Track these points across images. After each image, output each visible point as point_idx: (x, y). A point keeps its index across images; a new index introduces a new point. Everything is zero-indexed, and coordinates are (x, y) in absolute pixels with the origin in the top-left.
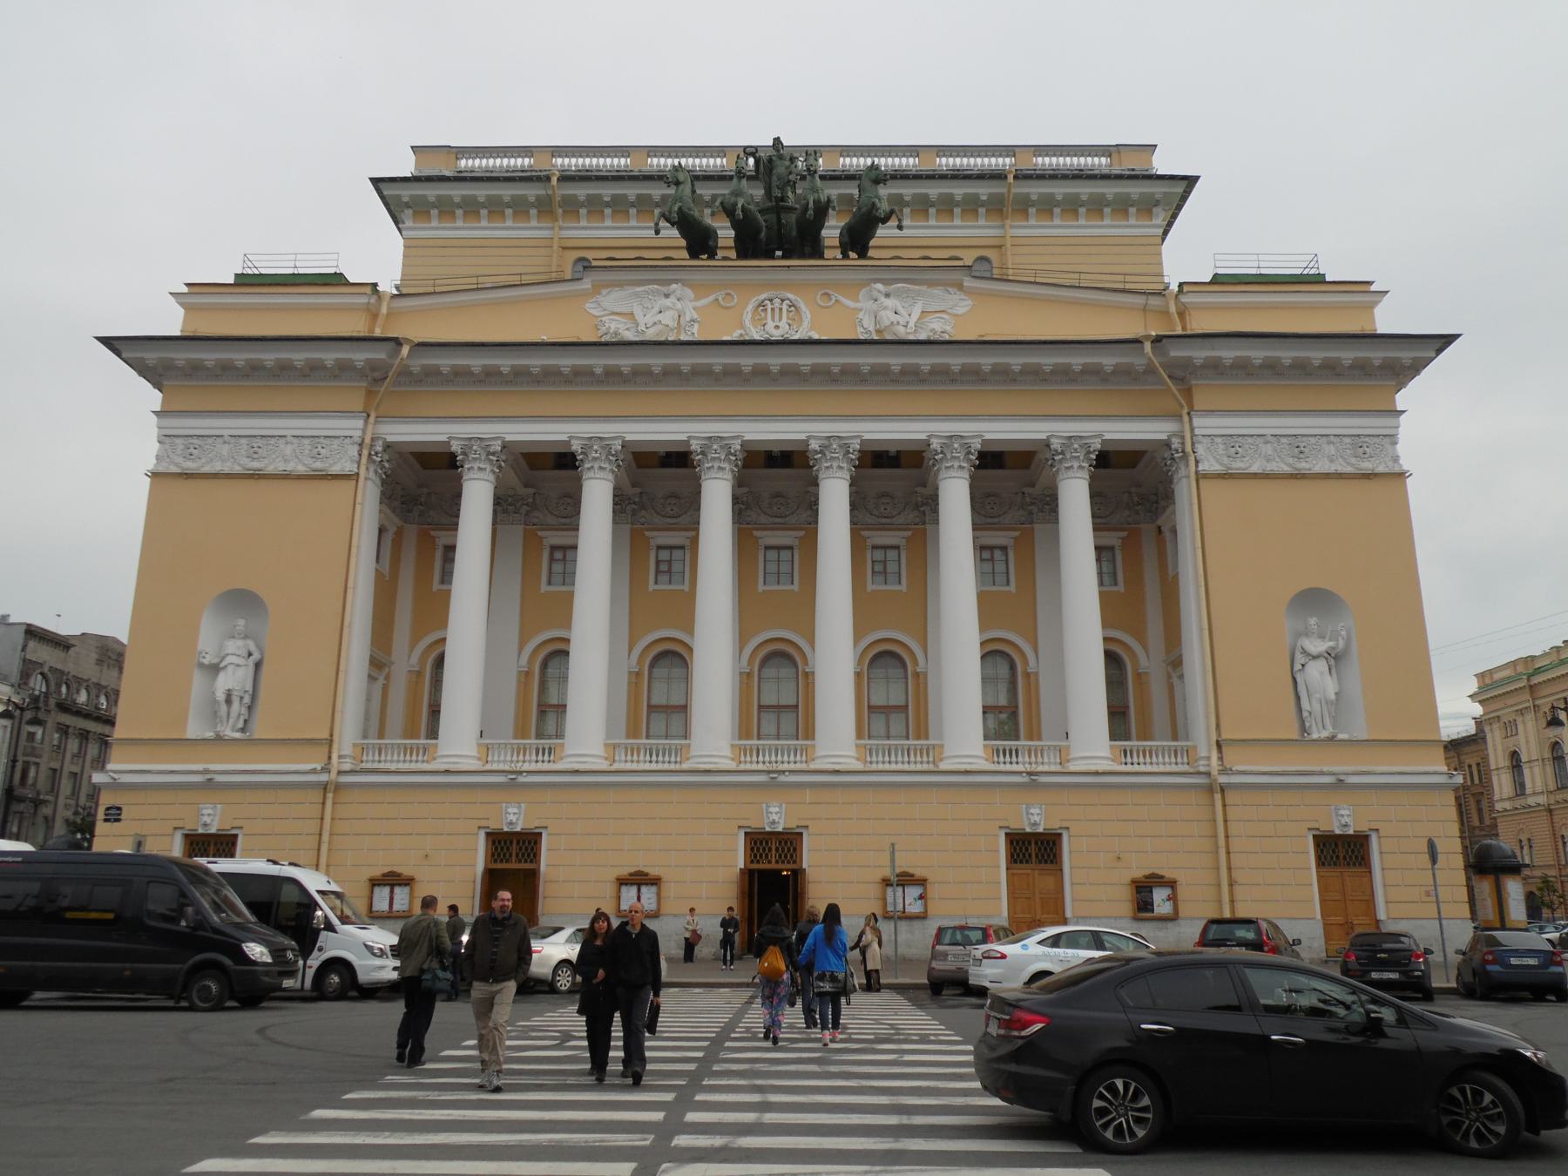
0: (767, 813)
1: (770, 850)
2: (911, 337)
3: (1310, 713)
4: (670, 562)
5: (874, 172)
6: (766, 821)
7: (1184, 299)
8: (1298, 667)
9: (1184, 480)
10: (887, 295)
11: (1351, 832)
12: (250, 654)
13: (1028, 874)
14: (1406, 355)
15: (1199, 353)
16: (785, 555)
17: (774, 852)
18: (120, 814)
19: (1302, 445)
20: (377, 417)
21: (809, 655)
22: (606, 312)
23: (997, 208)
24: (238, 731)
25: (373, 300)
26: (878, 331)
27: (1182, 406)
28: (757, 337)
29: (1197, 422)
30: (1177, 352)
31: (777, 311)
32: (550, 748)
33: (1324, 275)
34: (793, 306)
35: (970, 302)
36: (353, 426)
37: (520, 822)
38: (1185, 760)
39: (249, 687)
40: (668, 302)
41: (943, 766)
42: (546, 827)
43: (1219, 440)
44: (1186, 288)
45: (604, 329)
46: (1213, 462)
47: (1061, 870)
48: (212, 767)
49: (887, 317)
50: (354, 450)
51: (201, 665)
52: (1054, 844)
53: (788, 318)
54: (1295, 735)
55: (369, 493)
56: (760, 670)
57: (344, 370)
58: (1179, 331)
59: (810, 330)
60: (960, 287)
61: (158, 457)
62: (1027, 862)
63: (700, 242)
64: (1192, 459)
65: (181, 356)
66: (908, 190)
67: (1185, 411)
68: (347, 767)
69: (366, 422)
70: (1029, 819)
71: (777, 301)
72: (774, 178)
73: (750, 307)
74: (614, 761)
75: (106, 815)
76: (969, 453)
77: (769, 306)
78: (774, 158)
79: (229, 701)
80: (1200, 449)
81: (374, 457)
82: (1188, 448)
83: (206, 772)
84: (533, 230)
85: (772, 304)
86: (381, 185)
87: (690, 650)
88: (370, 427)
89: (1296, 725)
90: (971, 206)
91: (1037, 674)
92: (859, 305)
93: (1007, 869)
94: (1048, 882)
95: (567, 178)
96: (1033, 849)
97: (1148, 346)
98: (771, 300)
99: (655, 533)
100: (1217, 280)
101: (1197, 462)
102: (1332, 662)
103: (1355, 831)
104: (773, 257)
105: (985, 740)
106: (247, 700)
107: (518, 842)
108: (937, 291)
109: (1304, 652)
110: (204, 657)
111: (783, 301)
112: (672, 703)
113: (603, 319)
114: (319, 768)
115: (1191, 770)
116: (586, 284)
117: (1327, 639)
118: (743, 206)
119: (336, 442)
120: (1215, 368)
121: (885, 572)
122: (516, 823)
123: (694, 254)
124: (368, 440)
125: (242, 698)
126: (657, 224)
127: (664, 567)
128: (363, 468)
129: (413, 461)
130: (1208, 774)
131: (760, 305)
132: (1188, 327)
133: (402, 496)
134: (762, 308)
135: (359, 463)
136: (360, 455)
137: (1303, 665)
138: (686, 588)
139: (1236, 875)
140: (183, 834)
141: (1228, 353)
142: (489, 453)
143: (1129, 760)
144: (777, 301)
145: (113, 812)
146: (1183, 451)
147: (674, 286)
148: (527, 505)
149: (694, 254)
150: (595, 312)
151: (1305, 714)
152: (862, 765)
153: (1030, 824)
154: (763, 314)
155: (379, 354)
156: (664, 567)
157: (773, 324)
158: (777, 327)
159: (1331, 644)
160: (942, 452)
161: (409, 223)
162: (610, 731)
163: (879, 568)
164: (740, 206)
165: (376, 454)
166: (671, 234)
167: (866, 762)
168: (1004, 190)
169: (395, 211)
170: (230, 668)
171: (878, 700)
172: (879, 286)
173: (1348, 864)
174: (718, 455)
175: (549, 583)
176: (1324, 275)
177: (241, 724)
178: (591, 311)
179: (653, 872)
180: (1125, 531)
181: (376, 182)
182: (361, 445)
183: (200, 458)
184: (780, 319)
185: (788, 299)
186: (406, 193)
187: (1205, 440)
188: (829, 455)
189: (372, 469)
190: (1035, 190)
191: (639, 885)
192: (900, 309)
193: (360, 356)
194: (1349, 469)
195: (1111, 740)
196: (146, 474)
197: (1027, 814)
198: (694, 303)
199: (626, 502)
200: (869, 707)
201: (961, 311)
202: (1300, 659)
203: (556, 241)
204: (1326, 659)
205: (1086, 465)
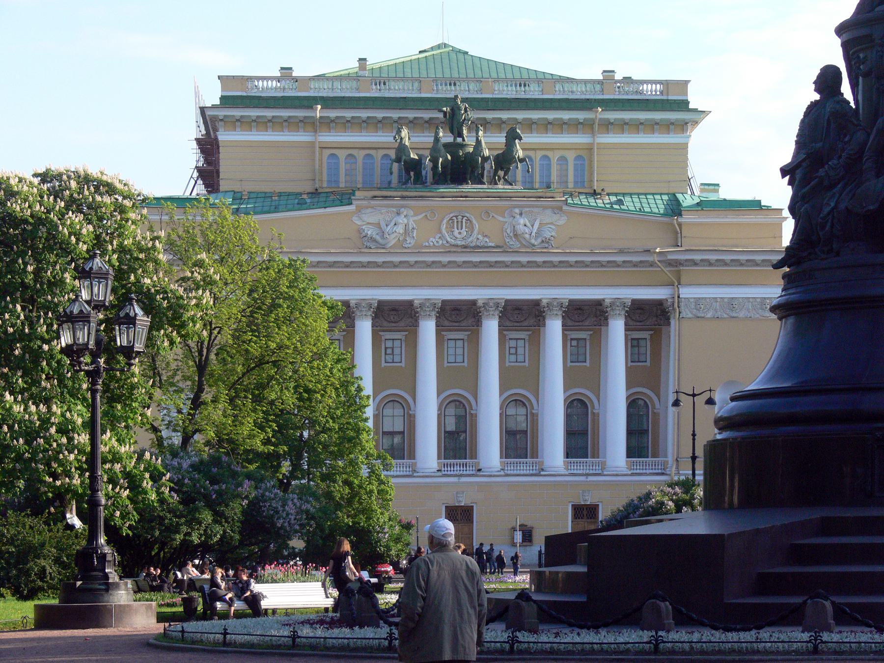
4: (393, 348)
16: (460, 343)
21: (474, 406)
23: (588, 126)
30: (670, 257)
43: (692, 300)
45: (364, 234)
46: (689, 313)
49: (520, 228)
60: (560, 209)
71: (460, 217)
73: (445, 221)
76: (562, 306)
80: (682, 304)
91: (598, 414)
96: (585, 512)
98: (456, 217)
111: (463, 217)
112: (395, 430)
113: (363, 227)
120: (694, 263)
127: (389, 351)
131: (450, 219)
141: (697, 257)
144: (460, 217)
150: (359, 223)
156: (389, 351)
158: (460, 233)
172: (517, 211)
178: (356, 222)
184: (462, 229)
192: (528, 224)
201: (561, 223)
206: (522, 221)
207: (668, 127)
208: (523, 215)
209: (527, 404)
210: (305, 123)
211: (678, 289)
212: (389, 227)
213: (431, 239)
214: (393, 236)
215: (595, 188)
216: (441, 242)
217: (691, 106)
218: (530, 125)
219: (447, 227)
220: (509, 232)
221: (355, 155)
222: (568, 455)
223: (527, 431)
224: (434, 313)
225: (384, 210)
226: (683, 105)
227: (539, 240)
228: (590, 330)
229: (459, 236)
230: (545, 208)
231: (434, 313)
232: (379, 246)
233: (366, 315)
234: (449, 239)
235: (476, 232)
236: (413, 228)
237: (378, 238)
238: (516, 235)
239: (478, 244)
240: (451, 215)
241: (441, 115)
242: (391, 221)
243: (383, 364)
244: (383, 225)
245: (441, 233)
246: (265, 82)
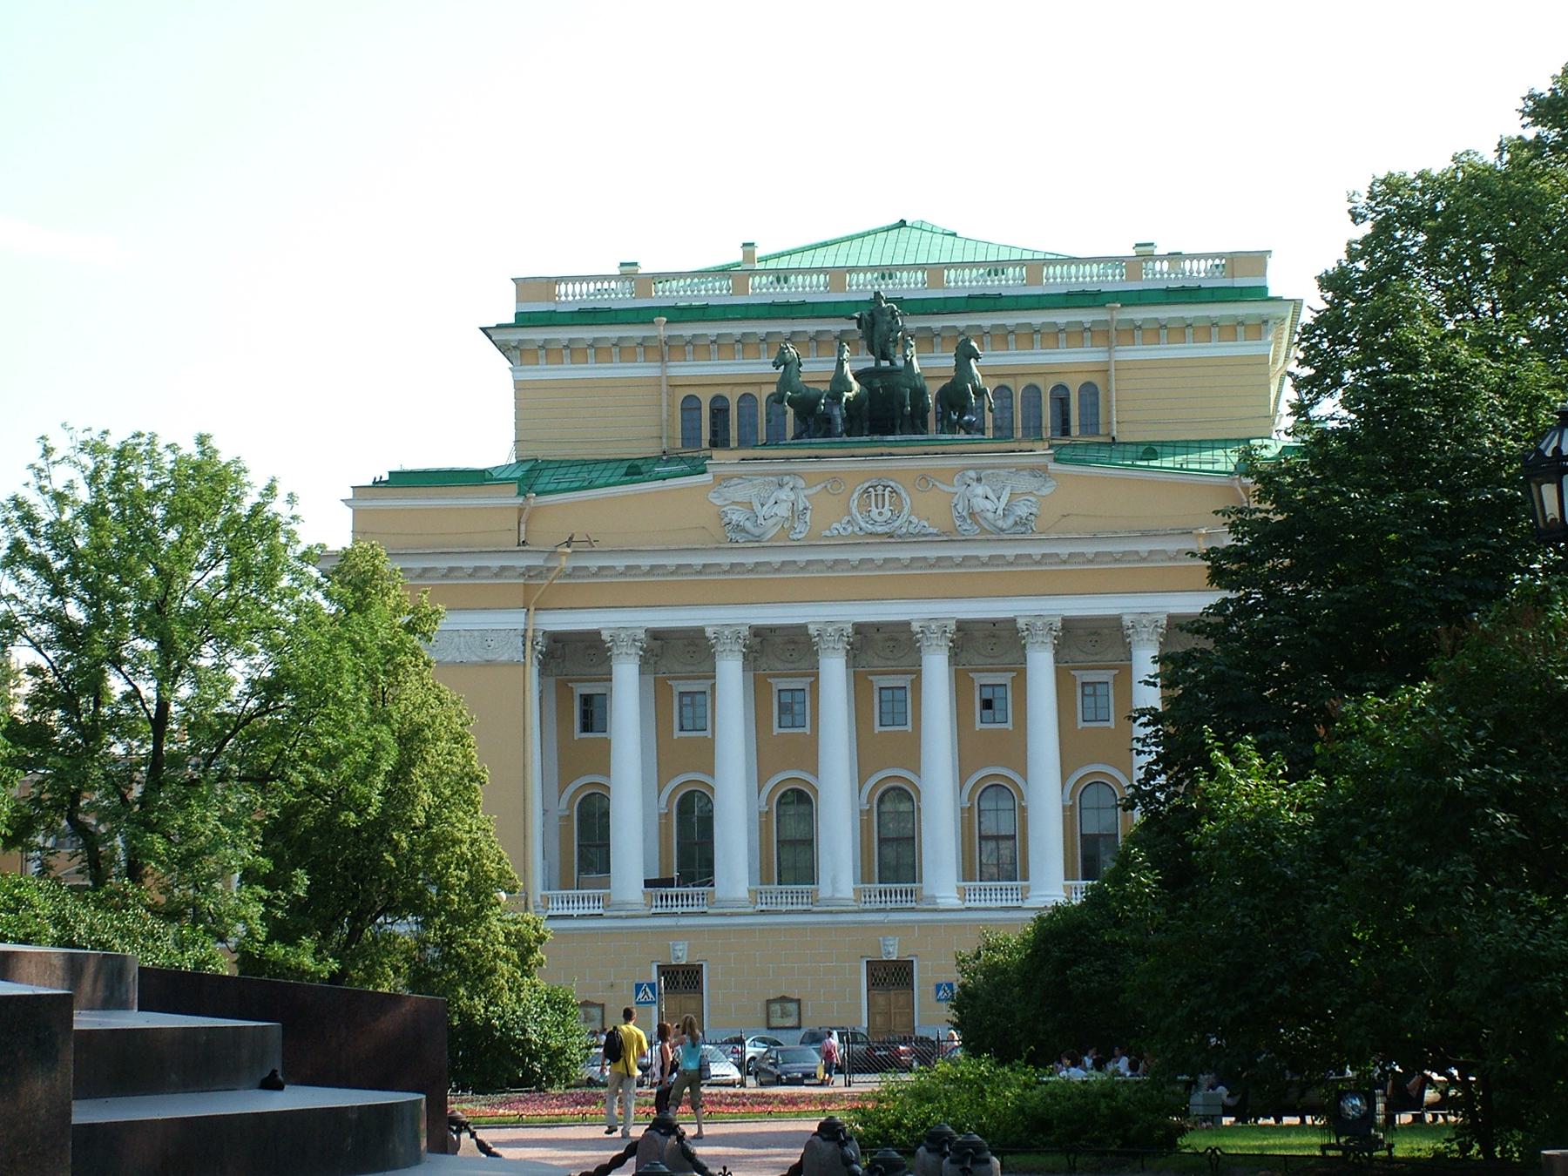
0: (884, 945)
6: (883, 952)
10: (979, 480)
22: (727, 502)
23: (1103, 335)
31: (880, 498)
34: (895, 491)
36: (514, 620)
45: (726, 520)
49: (979, 504)
55: (533, 671)
56: (878, 806)
69: (527, 614)
72: (876, 336)
73: (856, 495)
76: (1051, 629)
77: (873, 493)
84: (644, 370)
90: (1077, 334)
92: (951, 490)
98: (874, 487)
99: (777, 680)
107: (683, 972)
111: (885, 487)
119: (503, 633)
131: (865, 492)
135: (524, 652)
136: (524, 645)
138: (807, 730)
142: (634, 640)
144: (880, 488)
147: (787, 478)
150: (718, 502)
157: (878, 511)
158: (880, 514)
160: (1027, 629)
168: (1108, 318)
169: (504, 348)
171: (990, 827)
172: (972, 474)
175: (682, 729)
178: (714, 501)
181: (484, 330)
182: (524, 636)
186: (515, 336)
198: (806, 492)
201: (1045, 491)
203: (664, 378)
205: (1154, 637)
206: (980, 490)
207: (1233, 329)
208: (983, 481)
210: (1042, 334)
212: (765, 508)
213: (835, 525)
214: (771, 522)
215: (1114, 433)
216: (850, 529)
217: (1271, 294)
218: (1002, 337)
219: (859, 505)
220: (960, 511)
221: (1007, 384)
222: (967, 874)
224: (840, 645)
225: (760, 480)
226: (1258, 293)
227: (1010, 521)
228: (1114, 668)
229: (879, 519)
230: (1019, 469)
231: (840, 645)
232: (751, 538)
233: (731, 650)
234: (863, 525)
235: (906, 510)
236: (806, 509)
237: (748, 525)
238: (972, 515)
239: (911, 529)
240: (867, 485)
241: (853, 325)
242: (769, 497)
244: (757, 506)
245: (850, 514)
246: (570, 286)
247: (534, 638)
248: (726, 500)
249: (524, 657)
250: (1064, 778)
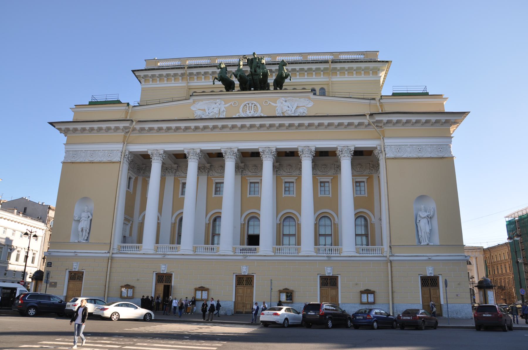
1: (244, 280)
2: (293, 115)
3: (421, 236)
5: (283, 62)
7: (381, 101)
8: (418, 221)
9: (382, 160)
11: (433, 275)
12: (89, 217)
13: (327, 289)
14: (452, 118)
15: (385, 118)
17: (245, 281)
18: (51, 265)
19: (420, 148)
20: (127, 144)
22: (197, 109)
24: (85, 240)
25: (127, 108)
26: (283, 113)
27: (381, 136)
28: (244, 116)
29: (385, 141)
32: (139, 247)
33: (428, 93)
34: (256, 105)
35: (313, 103)
36: (120, 147)
37: (166, 270)
38: (380, 252)
39: (88, 227)
40: (216, 106)
41: (342, 255)
42: (174, 272)
44: (383, 97)
45: (196, 115)
47: (338, 288)
48: (77, 251)
49: (285, 109)
50: (120, 154)
51: (74, 220)
52: (336, 279)
53: (254, 109)
54: (416, 242)
55: (125, 167)
57: (117, 129)
58: (381, 112)
59: (261, 113)
60: (309, 98)
61: (65, 157)
62: (327, 285)
63: (229, 86)
64: (384, 153)
65: (71, 127)
66: (297, 67)
67: (382, 137)
68: (115, 252)
69: (123, 145)
70: (327, 272)
71: (250, 105)
73: (242, 106)
74: (196, 252)
75: (47, 265)
78: (253, 59)
79: (82, 230)
80: (386, 149)
81: (126, 156)
82: (383, 150)
83: (75, 252)
85: (249, 105)
86: (135, 72)
87: (259, 215)
88: (124, 147)
89: (417, 240)
91: (338, 224)
93: (320, 288)
94: (333, 292)
95: (190, 67)
97: (368, 116)
98: (248, 104)
100: (394, 95)
101: (385, 154)
102: (429, 219)
103: (434, 275)
104: (250, 90)
105: (315, 246)
106: (88, 231)
108: (302, 100)
109: (420, 216)
110: (75, 218)
111: (252, 104)
114: (107, 252)
115: (382, 255)
116: (191, 101)
117: (428, 212)
118: (240, 75)
121: (289, 190)
122: (164, 271)
123: (227, 90)
124: (124, 151)
125: (86, 230)
126: (214, 81)
128: (122, 160)
129: (141, 157)
130: (386, 257)
131: (245, 106)
132: (383, 110)
133: (138, 168)
134: (245, 106)
136: (121, 156)
137: (419, 221)
139: (394, 289)
140: (69, 271)
143: (364, 252)
145: (49, 264)
146: (381, 151)
147: (218, 100)
148: (175, 170)
149: (227, 90)
150: (193, 109)
151: (420, 237)
152: (316, 254)
153: (327, 273)
154: (246, 108)
155: (127, 124)
158: (250, 112)
159: (428, 214)
161: (143, 83)
162: (195, 242)
163: (287, 189)
164: (239, 75)
165: (126, 156)
166: (219, 83)
167: (276, 253)
170: (83, 221)
172: (283, 99)
173: (432, 286)
174: (230, 154)
176: (428, 93)
177: (86, 238)
179: (206, 286)
180: (368, 176)
183: (76, 158)
184: (251, 110)
185: (254, 103)
186: (142, 74)
187: (389, 147)
188: (265, 153)
189: (125, 159)
190: (338, 66)
191: (202, 291)
192: (290, 106)
193: (121, 125)
194: (435, 156)
195: (315, 246)
196: (61, 163)
197: (327, 270)
198: (224, 106)
199: (206, 169)
200: (319, 234)
202: (418, 219)
204: (427, 218)
208: (287, 102)
209: (294, 218)
211: (383, 140)
212: (210, 110)
223: (295, 234)
240: (245, 103)
243: (214, 196)
247: (125, 153)
248: (196, 108)
249: (121, 160)
250: (315, 214)
